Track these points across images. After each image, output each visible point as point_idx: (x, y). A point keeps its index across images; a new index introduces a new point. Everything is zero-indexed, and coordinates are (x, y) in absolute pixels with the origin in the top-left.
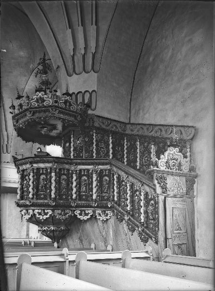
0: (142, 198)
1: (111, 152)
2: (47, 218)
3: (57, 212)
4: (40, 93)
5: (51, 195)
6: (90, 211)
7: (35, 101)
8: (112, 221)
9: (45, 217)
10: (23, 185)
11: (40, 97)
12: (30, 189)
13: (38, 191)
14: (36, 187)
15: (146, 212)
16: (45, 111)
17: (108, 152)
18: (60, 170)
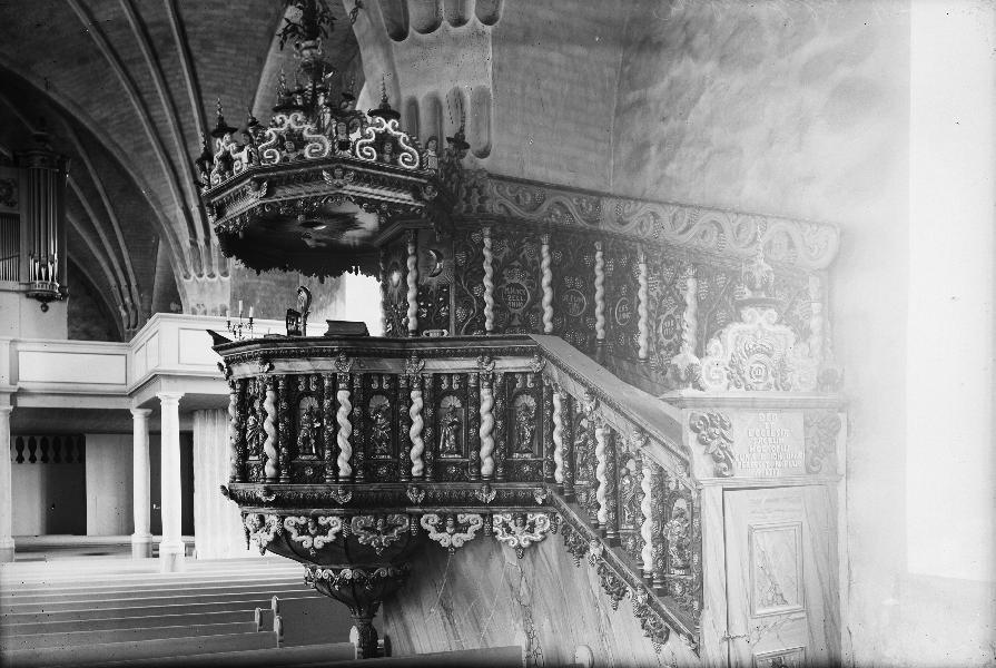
0: (646, 487)
1: (547, 298)
2: (326, 545)
3: (359, 522)
4: (288, 115)
5: (336, 469)
6: (472, 518)
7: (274, 146)
8: (552, 547)
9: (319, 541)
10: (245, 431)
11: (291, 130)
12: (268, 448)
13: (293, 451)
14: (287, 439)
15: (660, 539)
16: (307, 179)
17: (538, 296)
18: (367, 378)
